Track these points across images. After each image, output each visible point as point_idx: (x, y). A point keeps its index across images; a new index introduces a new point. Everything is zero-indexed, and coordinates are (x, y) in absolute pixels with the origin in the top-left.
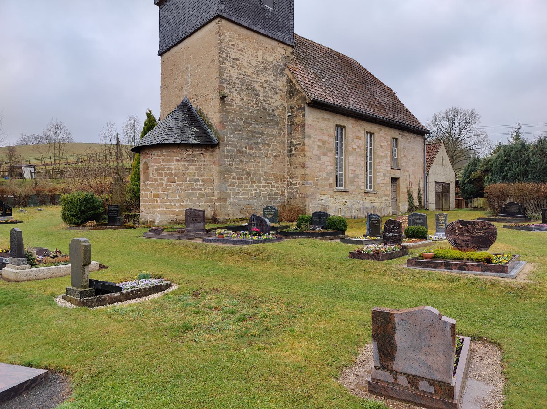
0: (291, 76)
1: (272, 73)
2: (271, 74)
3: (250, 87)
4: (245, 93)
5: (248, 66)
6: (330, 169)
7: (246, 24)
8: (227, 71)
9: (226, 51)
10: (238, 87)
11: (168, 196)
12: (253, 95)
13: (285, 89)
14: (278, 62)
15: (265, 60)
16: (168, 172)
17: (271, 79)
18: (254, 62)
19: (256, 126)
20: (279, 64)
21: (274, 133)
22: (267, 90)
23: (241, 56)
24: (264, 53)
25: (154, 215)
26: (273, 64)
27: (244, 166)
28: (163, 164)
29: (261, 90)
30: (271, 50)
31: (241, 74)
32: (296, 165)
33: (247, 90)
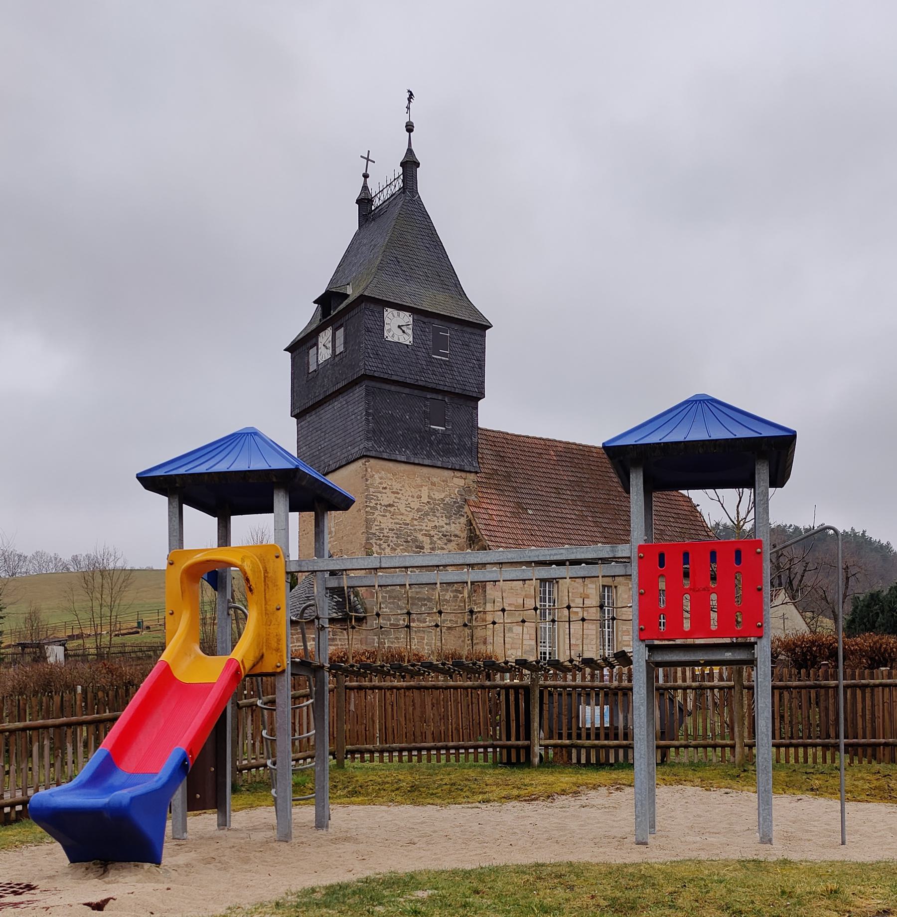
0: (471, 516)
1: (444, 515)
2: (442, 517)
3: (409, 539)
4: (401, 547)
5: (406, 510)
6: (530, 645)
7: (403, 458)
8: (376, 523)
9: (375, 498)
10: (392, 541)
12: (414, 549)
13: (464, 535)
14: (452, 498)
15: (432, 499)
17: (442, 523)
18: (415, 505)
19: (418, 590)
20: (455, 500)
21: (447, 597)
22: (435, 539)
23: (396, 500)
26: (446, 502)
27: (401, 644)
29: (427, 540)
30: (442, 483)
32: (478, 641)
33: (404, 543)
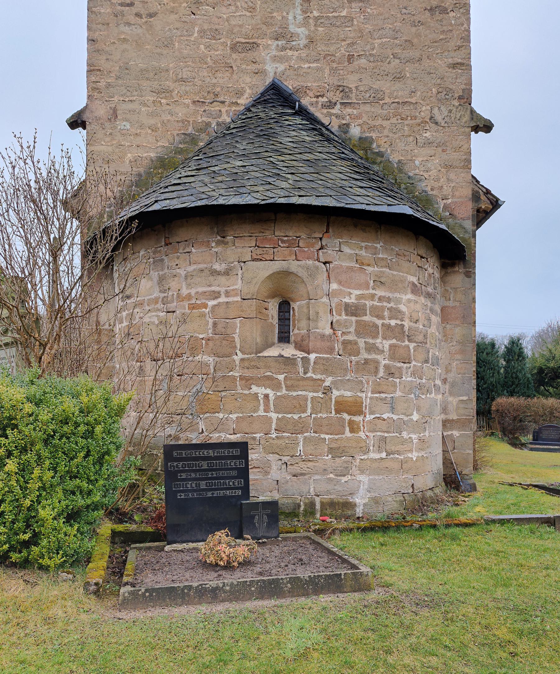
11: (393, 410)
16: (393, 322)
25: (344, 479)
28: (380, 293)
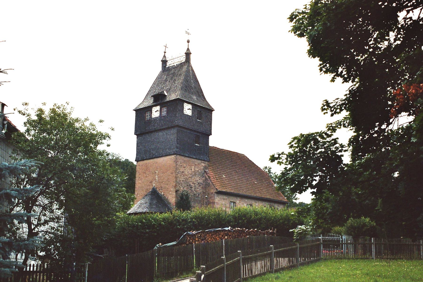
17: (198, 179)
24: (195, 167)
31: (185, 179)
